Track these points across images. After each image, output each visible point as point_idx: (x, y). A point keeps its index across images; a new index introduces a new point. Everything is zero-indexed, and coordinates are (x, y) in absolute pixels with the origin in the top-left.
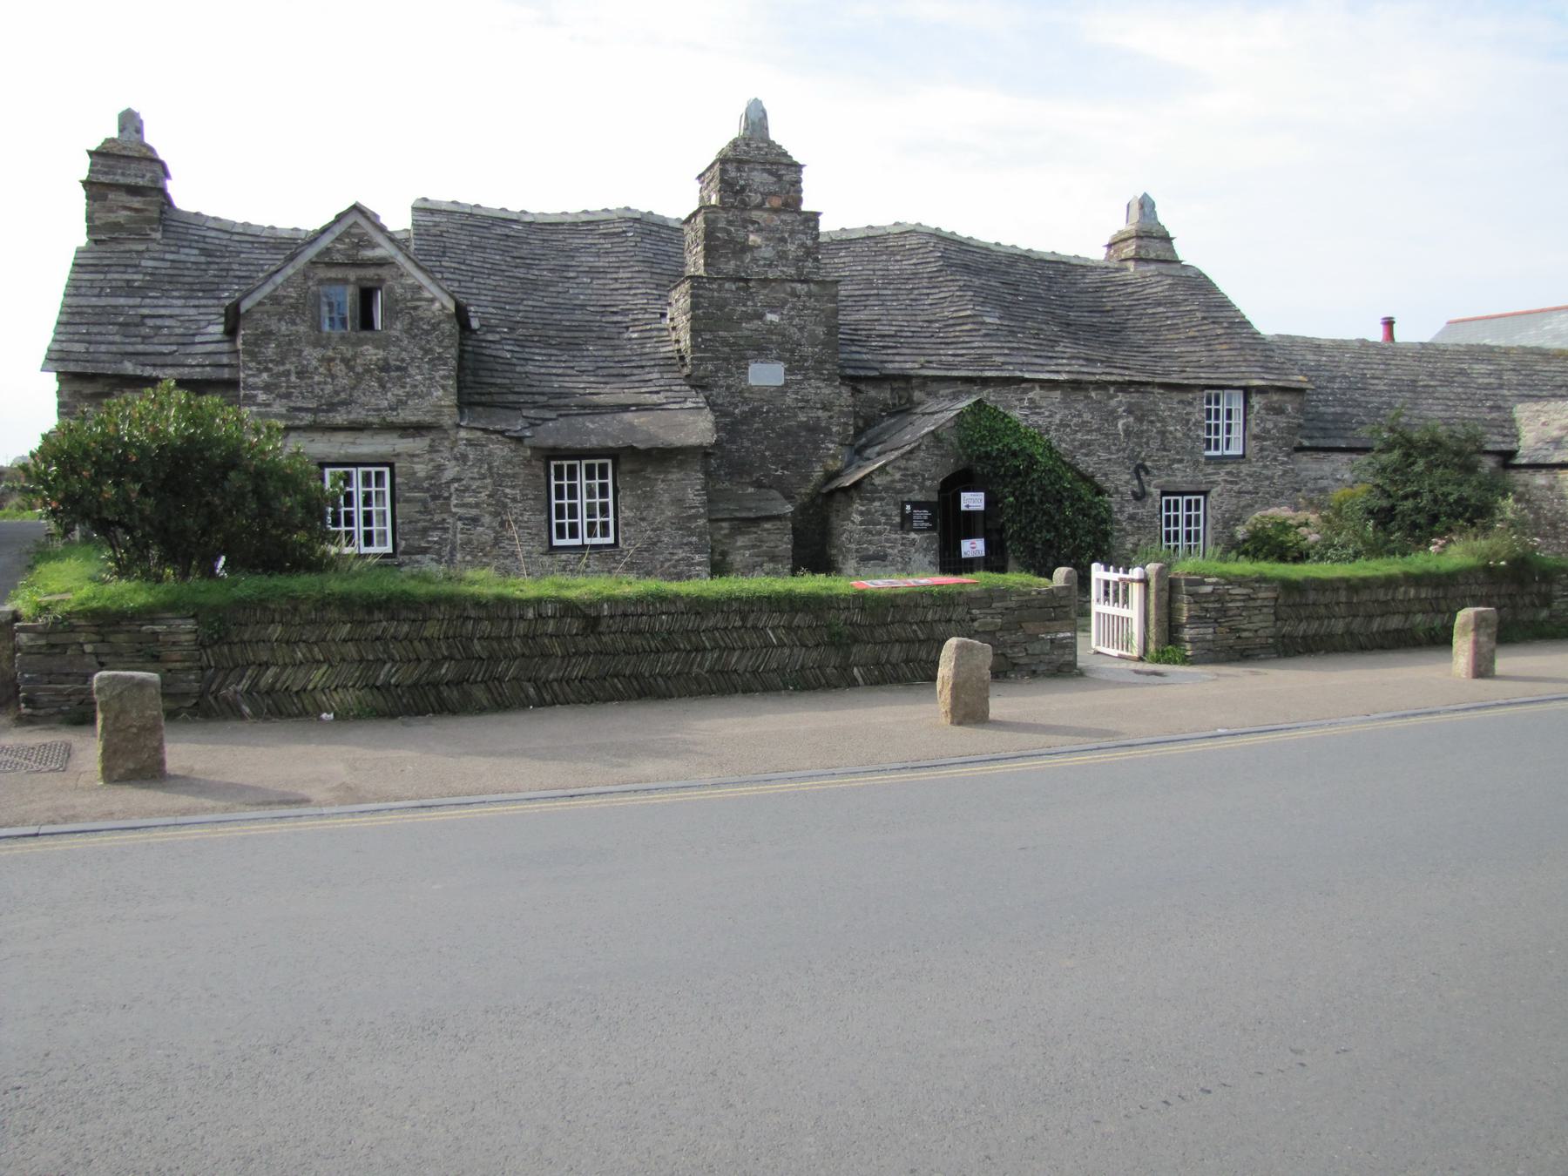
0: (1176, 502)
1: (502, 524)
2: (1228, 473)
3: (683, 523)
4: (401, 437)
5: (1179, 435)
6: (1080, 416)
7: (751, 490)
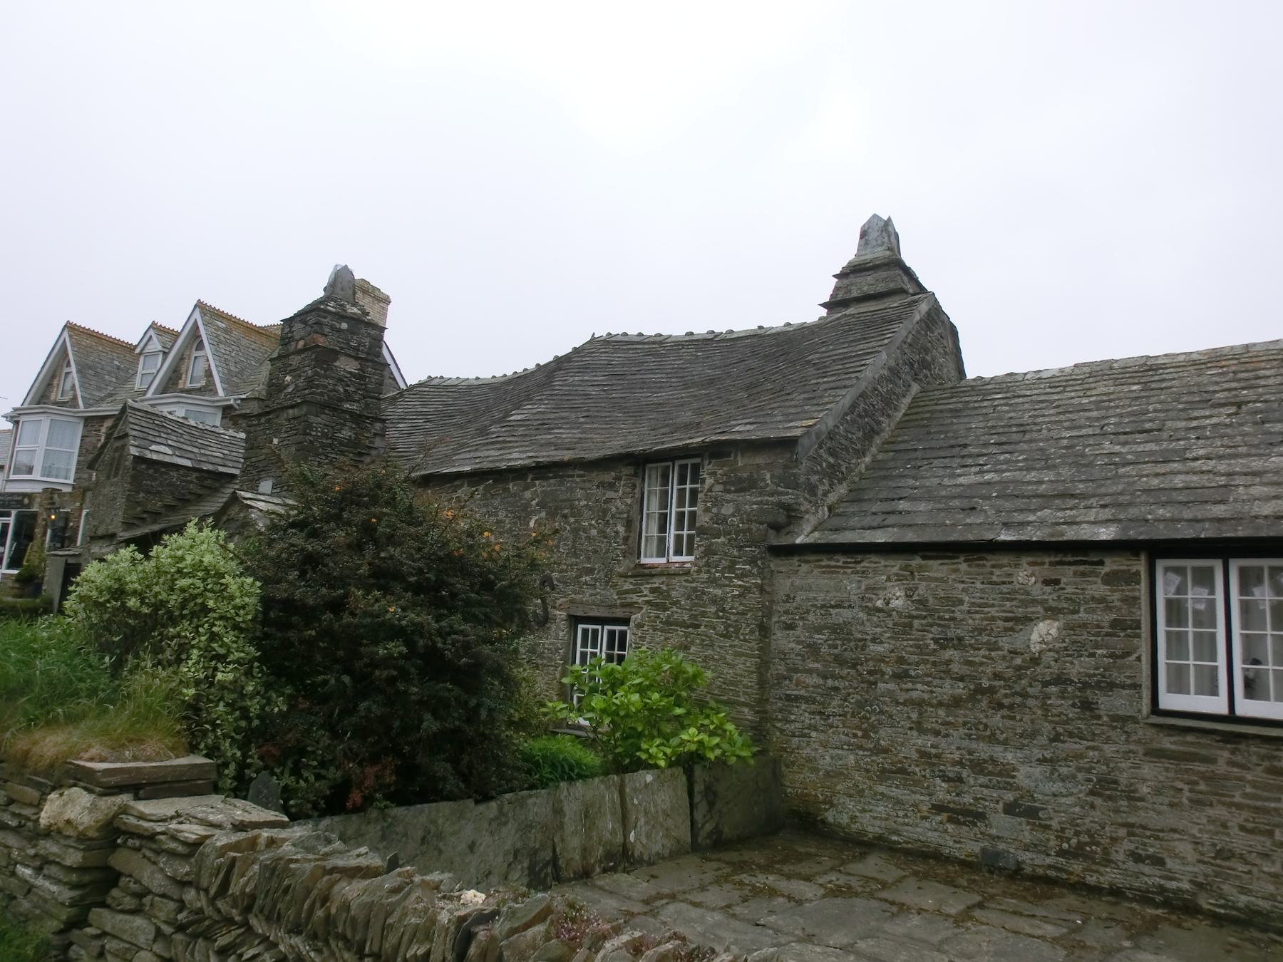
0: (595, 632)
2: (653, 591)
5: (594, 532)
6: (496, 514)
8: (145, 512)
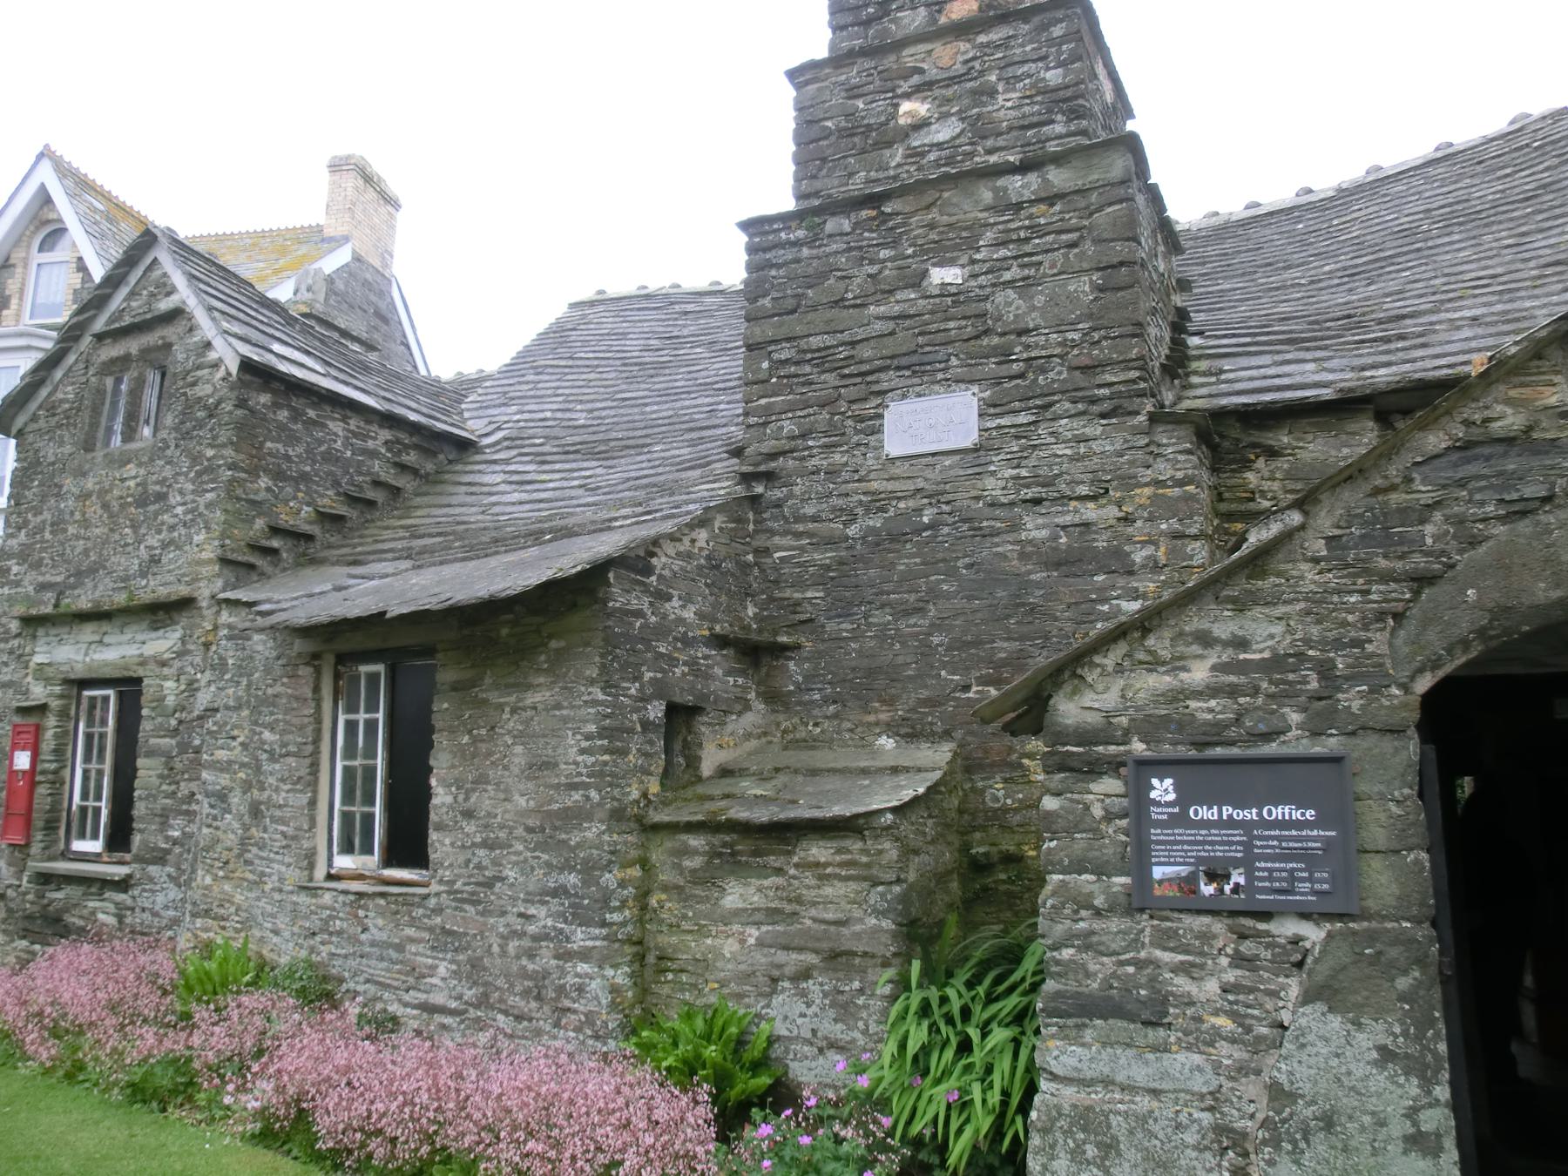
1: (256, 811)
3: (550, 829)
4: (155, 628)
7: (887, 743)
8: (275, 531)
